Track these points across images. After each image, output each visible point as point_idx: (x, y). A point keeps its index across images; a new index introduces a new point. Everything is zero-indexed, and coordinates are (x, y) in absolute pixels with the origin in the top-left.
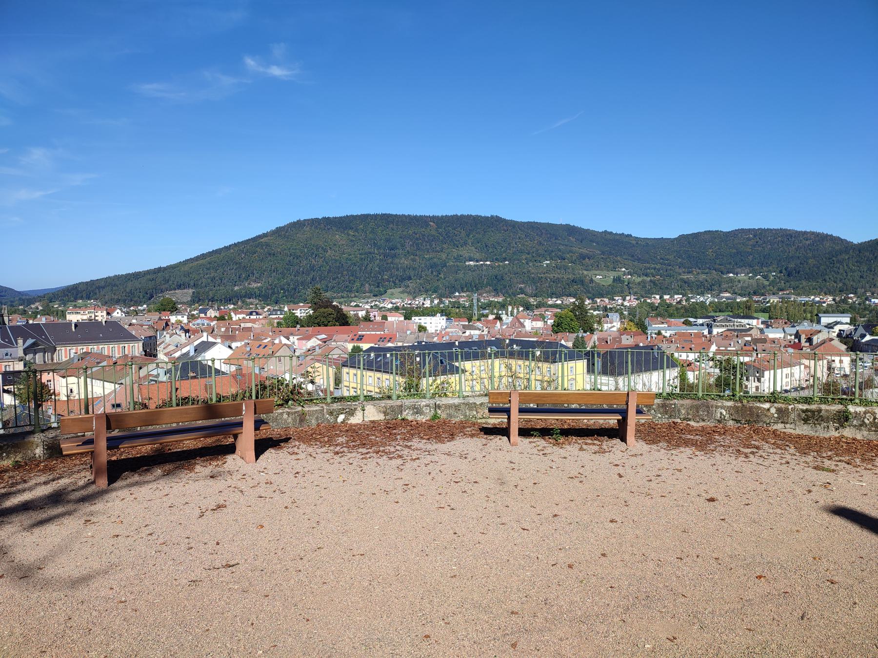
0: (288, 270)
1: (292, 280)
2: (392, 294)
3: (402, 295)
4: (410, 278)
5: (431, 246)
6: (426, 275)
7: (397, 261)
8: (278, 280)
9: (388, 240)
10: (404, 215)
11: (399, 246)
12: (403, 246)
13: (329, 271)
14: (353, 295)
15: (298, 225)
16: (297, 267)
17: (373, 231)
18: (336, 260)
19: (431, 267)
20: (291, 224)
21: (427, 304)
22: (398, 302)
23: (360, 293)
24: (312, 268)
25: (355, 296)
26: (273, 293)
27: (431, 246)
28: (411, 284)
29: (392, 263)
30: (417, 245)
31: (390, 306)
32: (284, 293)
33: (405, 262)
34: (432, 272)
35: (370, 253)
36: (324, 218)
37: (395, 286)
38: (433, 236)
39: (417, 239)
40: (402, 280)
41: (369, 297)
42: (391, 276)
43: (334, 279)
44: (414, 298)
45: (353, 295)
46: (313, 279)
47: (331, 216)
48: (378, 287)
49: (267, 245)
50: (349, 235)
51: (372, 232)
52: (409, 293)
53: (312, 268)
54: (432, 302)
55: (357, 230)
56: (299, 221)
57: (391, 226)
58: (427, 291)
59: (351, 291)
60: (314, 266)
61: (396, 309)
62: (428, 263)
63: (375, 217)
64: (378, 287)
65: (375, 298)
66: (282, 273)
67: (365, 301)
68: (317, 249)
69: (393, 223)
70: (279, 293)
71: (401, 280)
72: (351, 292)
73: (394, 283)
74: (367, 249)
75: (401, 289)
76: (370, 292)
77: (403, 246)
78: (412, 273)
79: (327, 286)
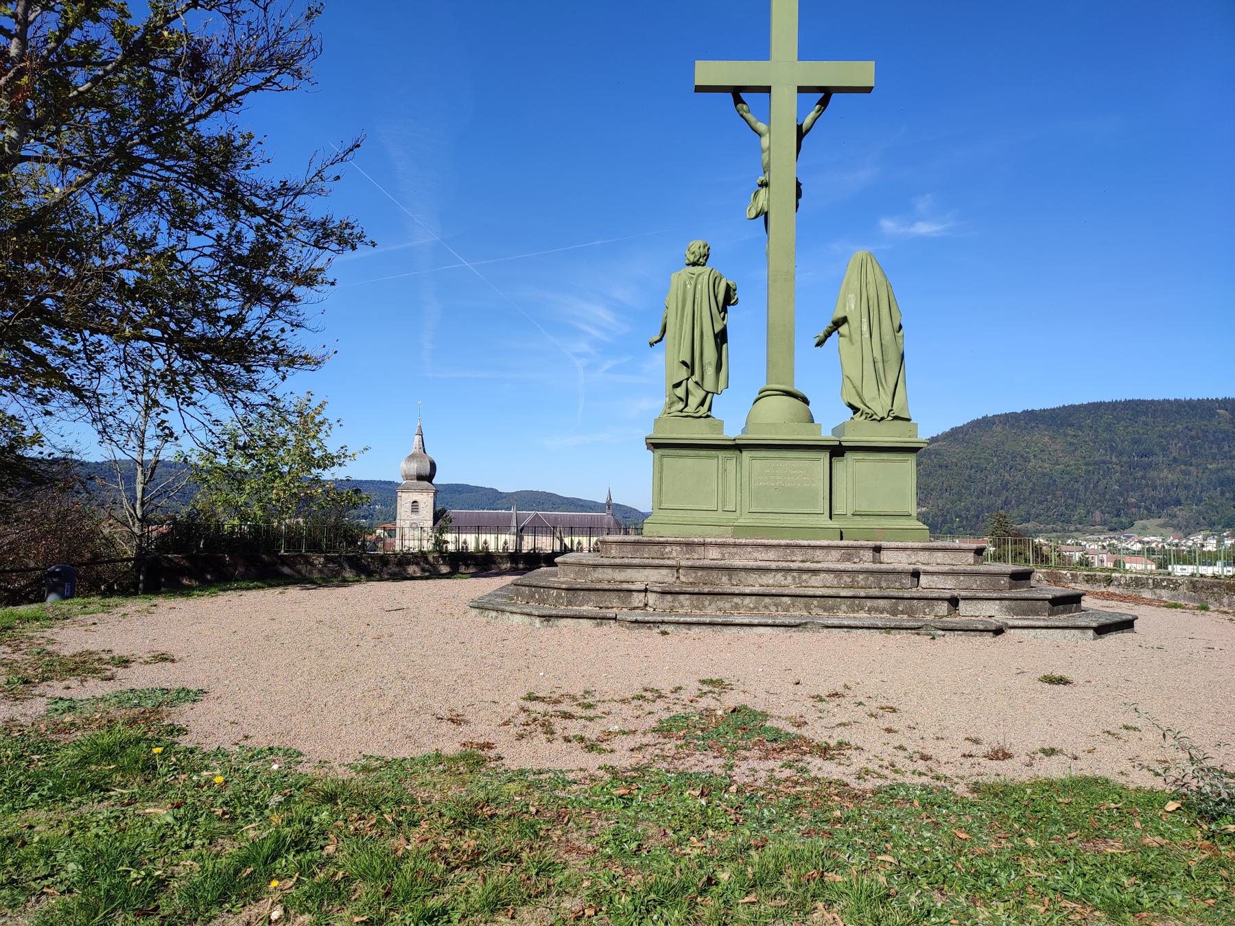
0: (967, 488)
1: (973, 503)
2: (1145, 528)
3: (1163, 530)
4: (1178, 502)
5: (1220, 448)
6: (1210, 497)
7: (1152, 474)
8: (952, 503)
9: (1136, 442)
10: (1168, 401)
11: (1157, 449)
12: (1164, 449)
13: (1033, 491)
14: (1072, 528)
15: (985, 424)
16: (981, 485)
17: (1109, 428)
18: (1044, 475)
19: (1221, 484)
20: (973, 422)
21: (1211, 546)
22: (1155, 541)
23: (1085, 525)
24: (1005, 486)
25: (1077, 530)
26: (945, 522)
27: (1220, 448)
28: (1181, 513)
29: (1143, 477)
30: (1193, 447)
31: (1138, 547)
32: (961, 522)
33: (1168, 476)
34: (1223, 493)
35: (1104, 462)
36: (1026, 412)
37: (1150, 514)
38: (1225, 432)
39: (1192, 438)
40: (1163, 505)
41: (1101, 532)
42: (1142, 498)
43: (1040, 503)
44: (1187, 536)
45: (1072, 528)
46: (1006, 503)
47: (1036, 408)
48: (1118, 515)
49: (937, 453)
50: (1066, 435)
51: (1109, 428)
52: (1177, 527)
53: (1005, 486)
54: (1220, 542)
55: (1080, 428)
56: (985, 418)
57: (1144, 418)
58: (1212, 525)
59: (1067, 521)
60: (1007, 483)
61: (1151, 551)
62: (1214, 477)
63: (1114, 405)
64: (1118, 515)
65: (1112, 534)
66: (958, 493)
67: (1095, 537)
68: (1014, 458)
69: (1145, 414)
70: (952, 522)
71: (1161, 506)
72: (1069, 522)
73: (1146, 508)
74: (1097, 457)
75: (1161, 521)
76: (1104, 523)
77: (1164, 449)
78: (1182, 494)
79: (1028, 513)
